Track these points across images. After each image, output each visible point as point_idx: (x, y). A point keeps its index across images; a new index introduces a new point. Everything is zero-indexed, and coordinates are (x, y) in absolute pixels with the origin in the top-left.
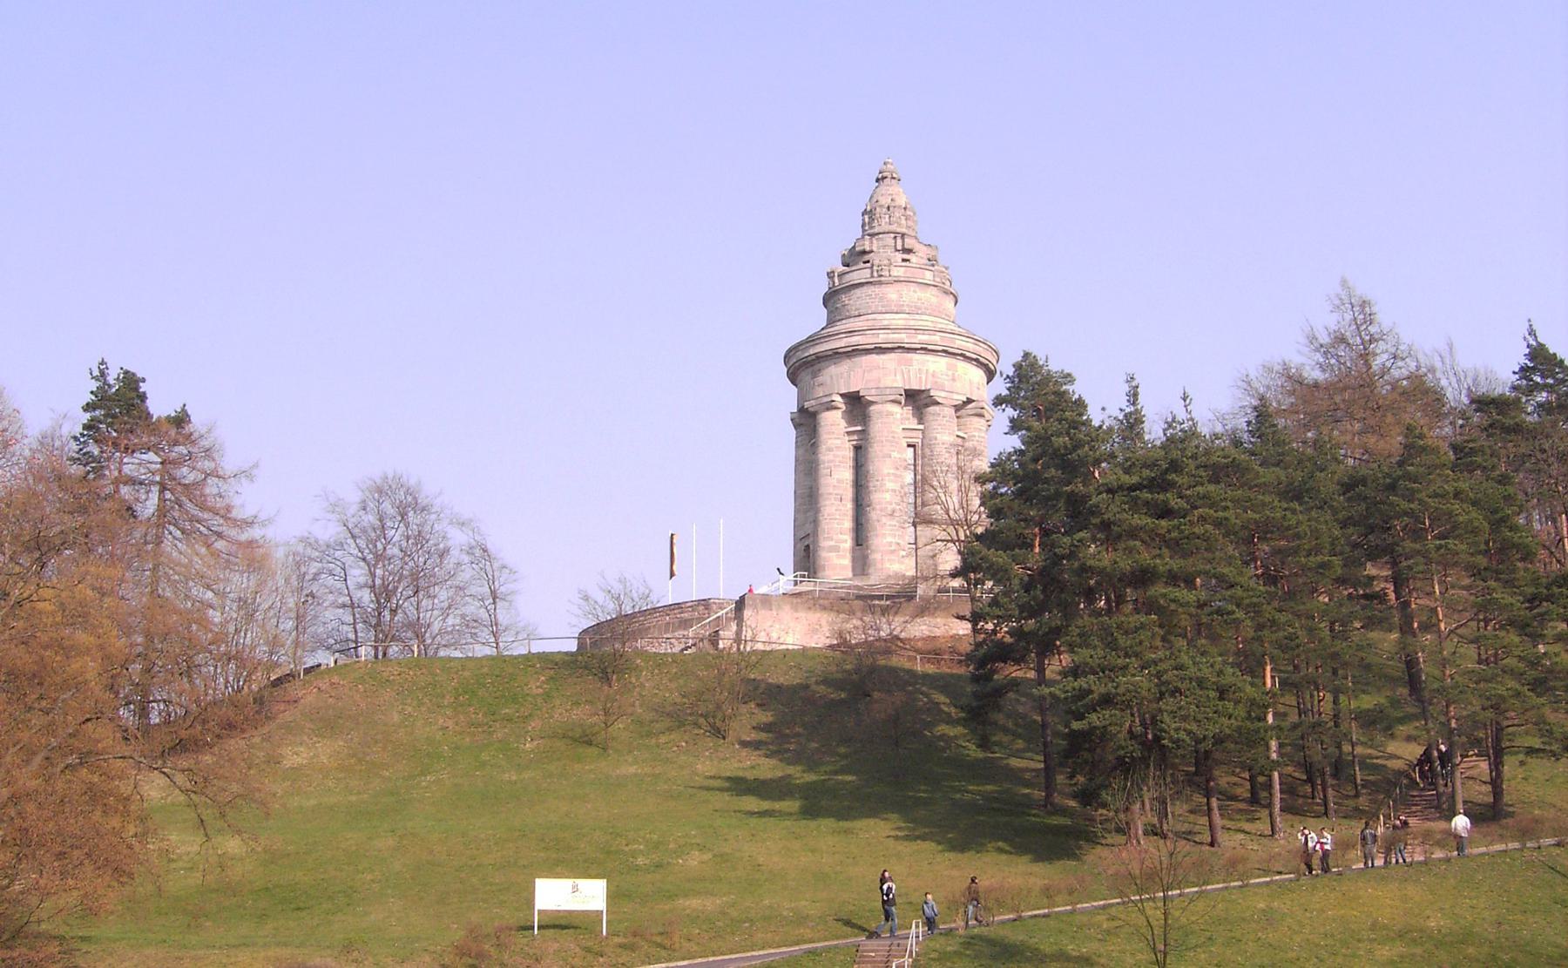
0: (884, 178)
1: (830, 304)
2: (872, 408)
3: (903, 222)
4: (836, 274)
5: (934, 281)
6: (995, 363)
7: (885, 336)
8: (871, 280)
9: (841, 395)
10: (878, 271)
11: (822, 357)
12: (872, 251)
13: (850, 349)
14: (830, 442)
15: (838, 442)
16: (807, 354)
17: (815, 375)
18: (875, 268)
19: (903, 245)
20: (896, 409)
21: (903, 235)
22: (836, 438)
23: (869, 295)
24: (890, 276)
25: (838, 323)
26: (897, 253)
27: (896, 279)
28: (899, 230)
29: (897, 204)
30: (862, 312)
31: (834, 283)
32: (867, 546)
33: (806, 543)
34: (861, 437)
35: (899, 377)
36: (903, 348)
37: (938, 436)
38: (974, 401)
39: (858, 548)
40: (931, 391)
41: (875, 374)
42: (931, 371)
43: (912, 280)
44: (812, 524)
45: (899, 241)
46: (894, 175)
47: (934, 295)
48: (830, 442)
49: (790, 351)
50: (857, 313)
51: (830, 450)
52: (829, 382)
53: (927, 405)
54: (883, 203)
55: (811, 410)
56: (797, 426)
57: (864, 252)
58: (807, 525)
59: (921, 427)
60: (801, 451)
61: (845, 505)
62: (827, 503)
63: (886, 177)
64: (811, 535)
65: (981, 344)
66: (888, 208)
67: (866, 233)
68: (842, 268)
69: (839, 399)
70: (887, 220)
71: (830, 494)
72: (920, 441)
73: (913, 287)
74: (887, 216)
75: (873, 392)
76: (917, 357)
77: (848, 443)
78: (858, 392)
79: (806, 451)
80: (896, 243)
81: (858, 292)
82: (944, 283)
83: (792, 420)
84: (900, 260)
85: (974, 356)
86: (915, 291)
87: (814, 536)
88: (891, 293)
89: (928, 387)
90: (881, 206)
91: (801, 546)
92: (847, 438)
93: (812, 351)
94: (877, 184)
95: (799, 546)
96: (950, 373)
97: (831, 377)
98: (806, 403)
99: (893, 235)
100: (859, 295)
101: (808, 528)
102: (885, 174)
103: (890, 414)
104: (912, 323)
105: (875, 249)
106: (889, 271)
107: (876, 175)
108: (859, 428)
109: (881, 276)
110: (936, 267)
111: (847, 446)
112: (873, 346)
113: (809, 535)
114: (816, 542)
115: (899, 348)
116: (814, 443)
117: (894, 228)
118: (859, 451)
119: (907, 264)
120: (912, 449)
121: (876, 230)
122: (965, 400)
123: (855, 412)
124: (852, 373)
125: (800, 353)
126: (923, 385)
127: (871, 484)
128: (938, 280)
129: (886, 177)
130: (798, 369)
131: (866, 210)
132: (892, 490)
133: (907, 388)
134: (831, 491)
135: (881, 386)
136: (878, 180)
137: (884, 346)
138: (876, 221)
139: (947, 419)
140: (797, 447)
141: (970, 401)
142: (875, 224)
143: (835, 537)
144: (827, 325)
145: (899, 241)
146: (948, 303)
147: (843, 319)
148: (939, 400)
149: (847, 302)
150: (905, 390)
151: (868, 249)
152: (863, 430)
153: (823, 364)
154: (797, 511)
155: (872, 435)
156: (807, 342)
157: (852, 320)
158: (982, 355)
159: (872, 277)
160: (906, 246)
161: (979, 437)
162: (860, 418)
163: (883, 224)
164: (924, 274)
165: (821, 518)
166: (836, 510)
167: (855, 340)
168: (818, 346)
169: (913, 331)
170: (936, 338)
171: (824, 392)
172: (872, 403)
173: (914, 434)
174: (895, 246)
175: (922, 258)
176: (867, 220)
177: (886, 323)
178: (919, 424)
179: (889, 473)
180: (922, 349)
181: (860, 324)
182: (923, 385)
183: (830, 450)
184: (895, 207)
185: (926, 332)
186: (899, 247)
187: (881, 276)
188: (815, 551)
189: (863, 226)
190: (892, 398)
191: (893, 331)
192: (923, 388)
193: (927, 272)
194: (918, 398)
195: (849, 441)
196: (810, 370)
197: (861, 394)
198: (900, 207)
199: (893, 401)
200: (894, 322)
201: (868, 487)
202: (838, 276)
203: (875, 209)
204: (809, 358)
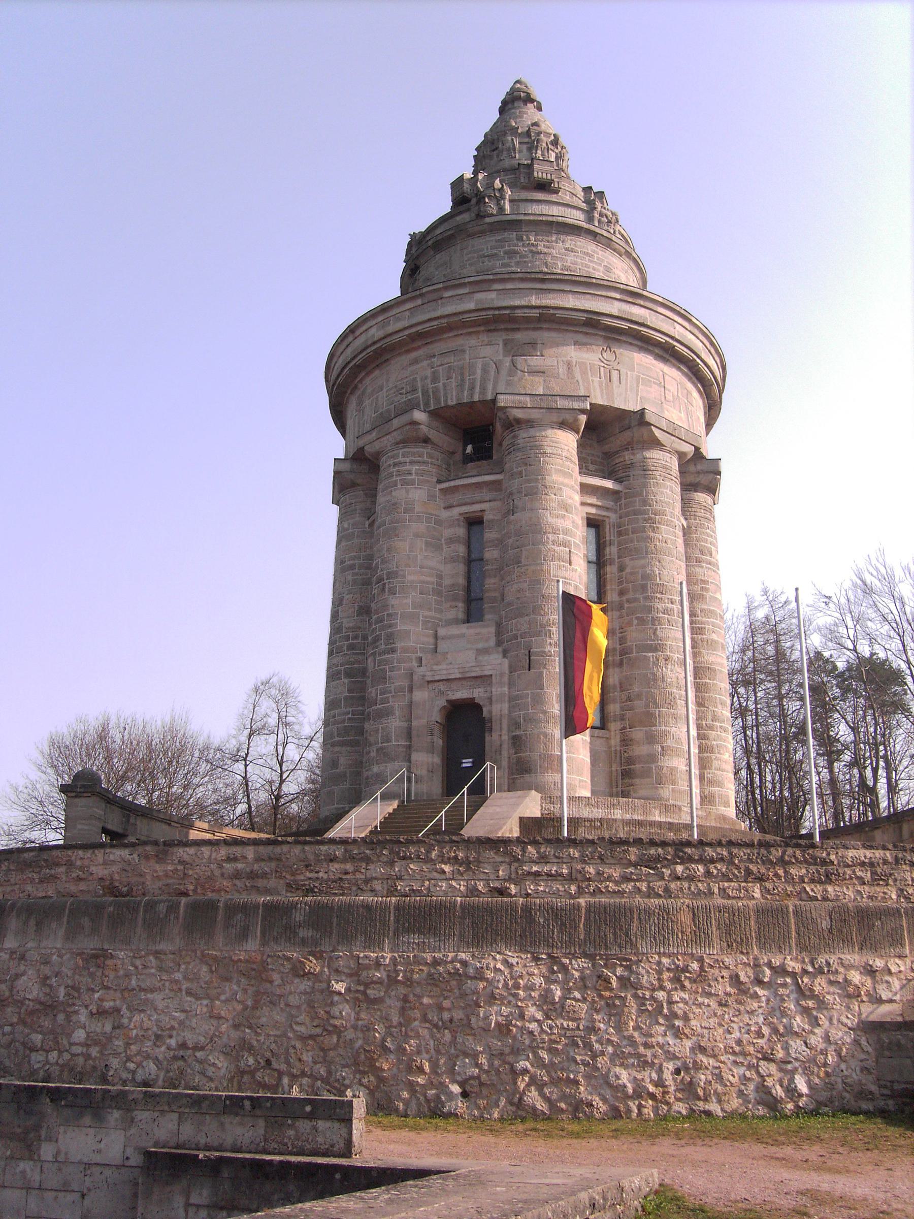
7: (682, 330)
13: (625, 325)
17: (515, 350)
34: (610, 504)
93: (534, 300)
112: (662, 338)
124: (615, 374)
125: (493, 295)
167: (637, 312)
168: (551, 296)
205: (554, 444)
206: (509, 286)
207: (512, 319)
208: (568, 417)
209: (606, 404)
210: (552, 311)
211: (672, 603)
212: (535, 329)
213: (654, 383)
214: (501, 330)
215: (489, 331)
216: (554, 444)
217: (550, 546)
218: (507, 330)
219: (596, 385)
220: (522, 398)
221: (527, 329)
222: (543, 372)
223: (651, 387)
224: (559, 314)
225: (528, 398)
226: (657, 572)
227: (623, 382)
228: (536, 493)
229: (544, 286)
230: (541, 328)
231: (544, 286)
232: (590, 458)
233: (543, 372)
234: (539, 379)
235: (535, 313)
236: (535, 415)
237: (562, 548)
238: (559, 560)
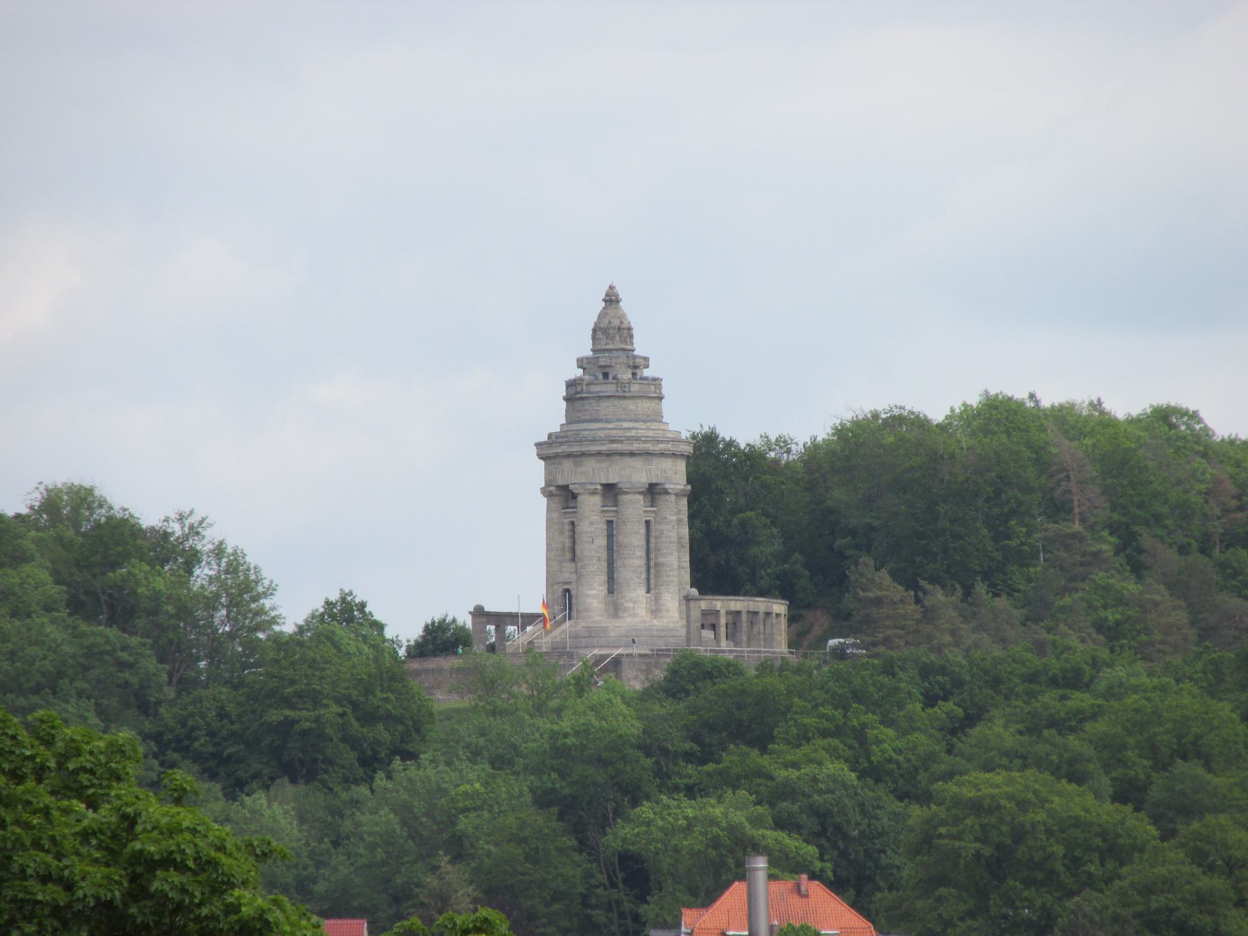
7: (638, 445)
18: (619, 384)
20: (640, 497)
24: (630, 391)
37: (668, 516)
53: (660, 494)
55: (575, 491)
74: (618, 336)
76: (656, 461)
88: (630, 405)
89: (663, 481)
90: (614, 328)
91: (559, 590)
109: (624, 391)
148: (670, 491)
152: (616, 511)
167: (615, 446)
170: (669, 446)
172: (626, 493)
173: (649, 514)
178: (652, 506)
190: (641, 490)
236: (581, 491)
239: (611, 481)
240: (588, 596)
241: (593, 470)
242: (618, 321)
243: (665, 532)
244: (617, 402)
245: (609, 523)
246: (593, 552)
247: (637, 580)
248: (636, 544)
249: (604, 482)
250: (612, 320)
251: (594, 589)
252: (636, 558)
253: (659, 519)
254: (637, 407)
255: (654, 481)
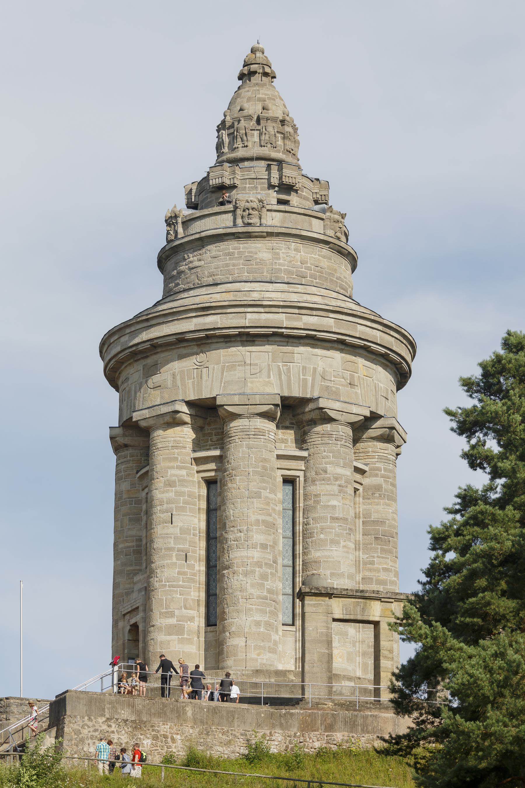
0: (252, 73)
1: (169, 265)
2: (233, 424)
3: (280, 142)
4: (180, 220)
5: (324, 234)
6: (408, 358)
8: (234, 230)
9: (189, 404)
10: (242, 217)
11: (161, 346)
12: (233, 187)
14: (170, 472)
15: (184, 472)
16: (137, 340)
18: (239, 212)
19: (281, 178)
21: (280, 163)
22: (179, 468)
23: (229, 254)
25: (185, 295)
26: (271, 192)
27: (269, 230)
28: (274, 155)
29: (270, 114)
30: (219, 278)
31: (176, 233)
32: (224, 627)
33: (133, 621)
35: (273, 378)
36: (281, 335)
37: (330, 468)
38: (380, 417)
39: (209, 628)
40: (320, 400)
41: (239, 373)
42: (320, 369)
43: (294, 232)
44: (143, 593)
45: (275, 174)
46: (267, 70)
47: (324, 257)
48: (170, 472)
49: (111, 334)
50: (210, 280)
51: (170, 484)
52: (169, 383)
54: (251, 112)
55: (143, 424)
56: (117, 448)
57: (222, 188)
58: (135, 595)
59: (305, 454)
60: (125, 486)
61: (192, 567)
62: (165, 562)
63: (255, 73)
64: (141, 608)
65: (392, 333)
66: (258, 121)
67: (224, 158)
68: (188, 212)
69: (185, 409)
70: (257, 139)
71: (171, 549)
72: (301, 474)
73: (293, 244)
74: (256, 133)
75: (236, 400)
77: (196, 475)
78: (215, 398)
79: (133, 485)
80: (269, 174)
81: (213, 249)
82: (338, 239)
83: (112, 438)
84: (275, 201)
85: (383, 350)
86: (297, 250)
87: (145, 610)
89: (316, 395)
90: (249, 117)
91: (125, 626)
92: (195, 468)
93: (145, 336)
94: (240, 82)
95: (121, 624)
96: (347, 374)
97: (174, 375)
98: (134, 414)
99: (263, 163)
100: (214, 253)
101: (136, 599)
102: (253, 67)
103: (259, 433)
104: (294, 298)
105: (237, 182)
106: (260, 218)
107: (239, 67)
108: (217, 453)
109: (249, 224)
110: (328, 214)
111: (196, 479)
113: (137, 608)
114: (147, 619)
115: (275, 334)
116: (147, 472)
117: (266, 151)
118: (212, 486)
119: (282, 207)
120: (289, 488)
121: (241, 153)
122: (368, 414)
123: (207, 428)
126: (309, 391)
127: (231, 536)
128: (331, 233)
129: (255, 73)
130: (123, 363)
131: (223, 122)
132: (262, 544)
133: (286, 394)
134: (172, 545)
135: (248, 391)
136: (241, 77)
137: (252, 331)
138: (239, 139)
139: (343, 442)
140: (118, 479)
141: (374, 417)
142: (239, 144)
143: (177, 612)
144: (163, 299)
145: (275, 174)
146: (344, 265)
147: (191, 289)
148: (332, 414)
149: (196, 264)
150: (281, 397)
151: (227, 182)
153: (162, 355)
154: (117, 573)
155: (233, 464)
156: (138, 323)
157: (203, 291)
158: (394, 348)
159: (235, 225)
160: (285, 180)
161: (385, 470)
162: (215, 438)
163: (250, 144)
164: (311, 224)
165: (157, 585)
166: (179, 573)
168: (153, 329)
169: (296, 311)
171: (162, 397)
174: (269, 179)
175: (306, 199)
176: (226, 140)
177: (255, 296)
178: (301, 449)
179: (258, 520)
180: (308, 337)
181: (218, 297)
182: (309, 391)
183: (170, 484)
184: (267, 119)
185: (314, 313)
186: (275, 181)
187: (249, 224)
188: (146, 633)
189: (219, 146)
190: (265, 408)
191: (267, 310)
192: (308, 396)
193: (314, 221)
194: (299, 411)
195: (198, 472)
196: (143, 362)
197: (218, 402)
198: (274, 119)
199: (263, 415)
200: (267, 295)
201: (226, 539)
202: (183, 223)
203: (239, 121)
204: (140, 347)
205: (164, 440)
206: (133, 329)
207: (141, 352)
208: (167, 419)
209: (196, 398)
210: (155, 341)
211: (241, 532)
212: (155, 354)
213: (239, 365)
214: (139, 359)
215: (136, 361)
216: (164, 440)
217: (158, 515)
218: (143, 358)
219: (190, 385)
220: (144, 411)
221: (151, 355)
222: (160, 386)
223: (235, 370)
224: (159, 341)
225: (147, 411)
226: (232, 512)
227: (211, 376)
228: (153, 479)
229: (149, 324)
230: (158, 352)
231: (149, 324)
232: (214, 432)
233: (160, 386)
234: (157, 392)
235: (147, 345)
236: (151, 422)
237: (165, 514)
238: (163, 523)
239: (206, 394)
240: (160, 629)
241: (174, 375)
242: (259, 107)
243: (323, 499)
244: (231, 245)
245: (210, 483)
246: (172, 541)
247: (255, 592)
248: (253, 518)
249: (192, 397)
250: (246, 105)
251: (171, 615)
252: (254, 547)
253: (312, 474)
254: (276, 256)
255: (296, 392)
